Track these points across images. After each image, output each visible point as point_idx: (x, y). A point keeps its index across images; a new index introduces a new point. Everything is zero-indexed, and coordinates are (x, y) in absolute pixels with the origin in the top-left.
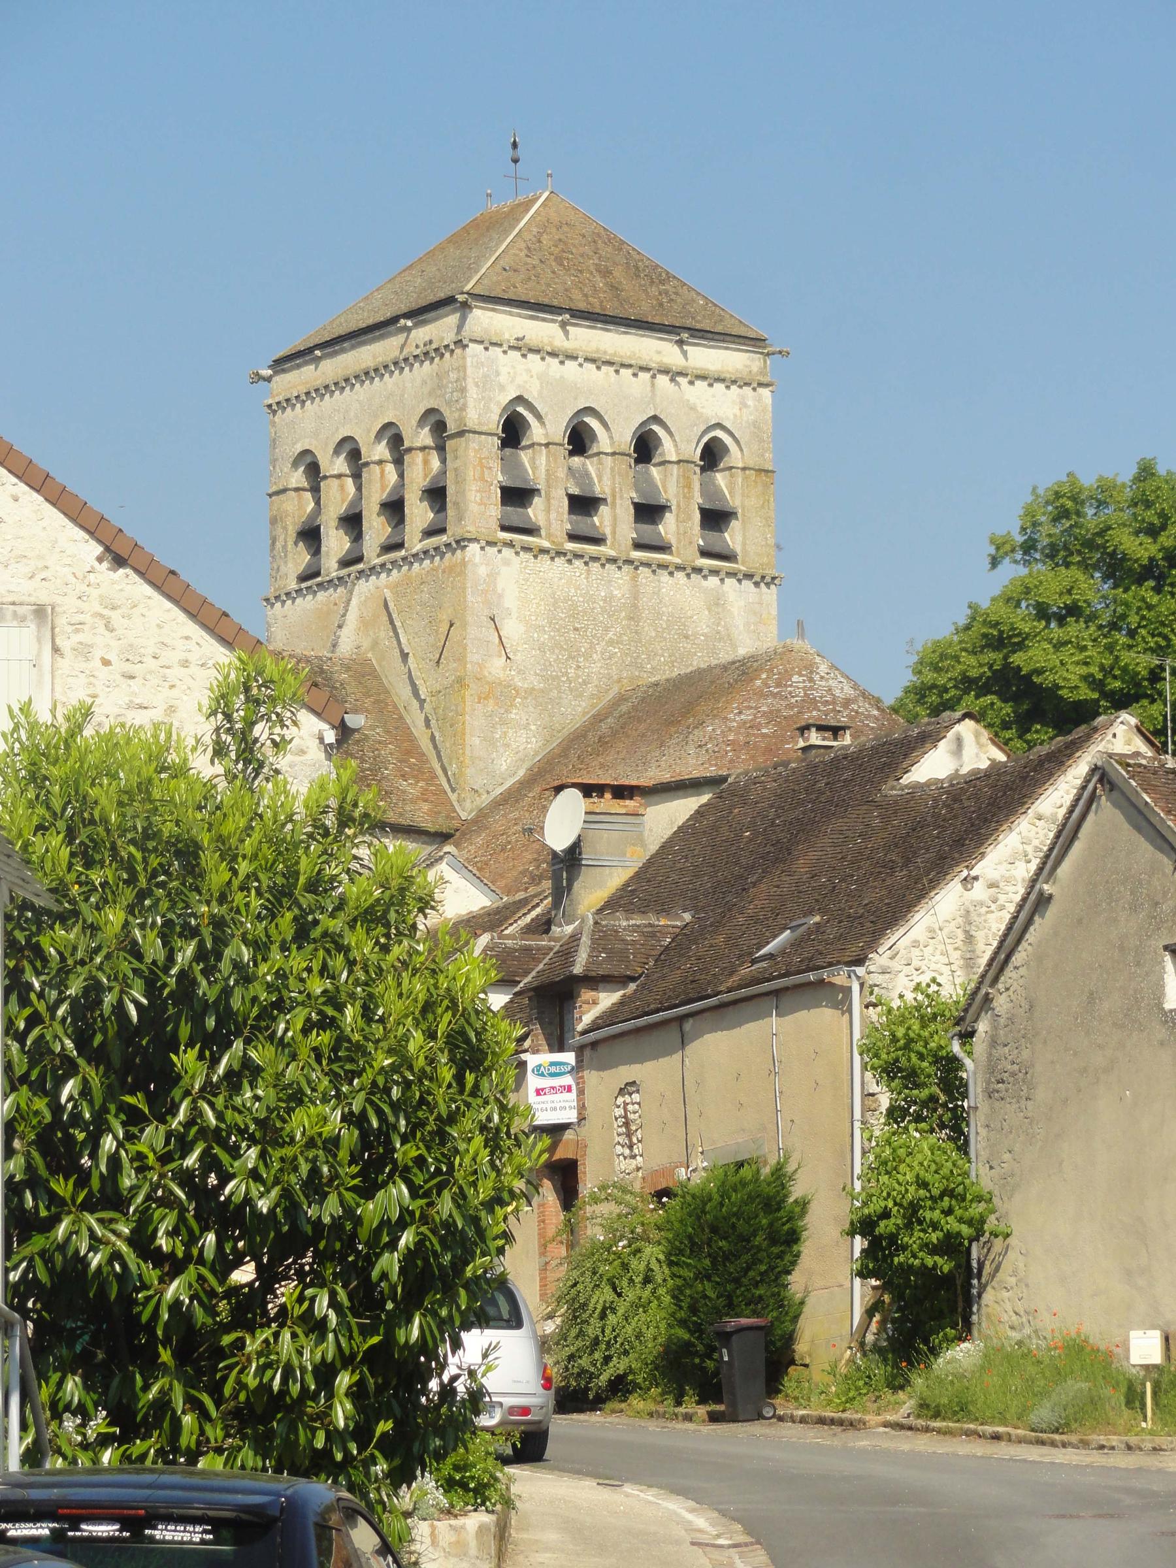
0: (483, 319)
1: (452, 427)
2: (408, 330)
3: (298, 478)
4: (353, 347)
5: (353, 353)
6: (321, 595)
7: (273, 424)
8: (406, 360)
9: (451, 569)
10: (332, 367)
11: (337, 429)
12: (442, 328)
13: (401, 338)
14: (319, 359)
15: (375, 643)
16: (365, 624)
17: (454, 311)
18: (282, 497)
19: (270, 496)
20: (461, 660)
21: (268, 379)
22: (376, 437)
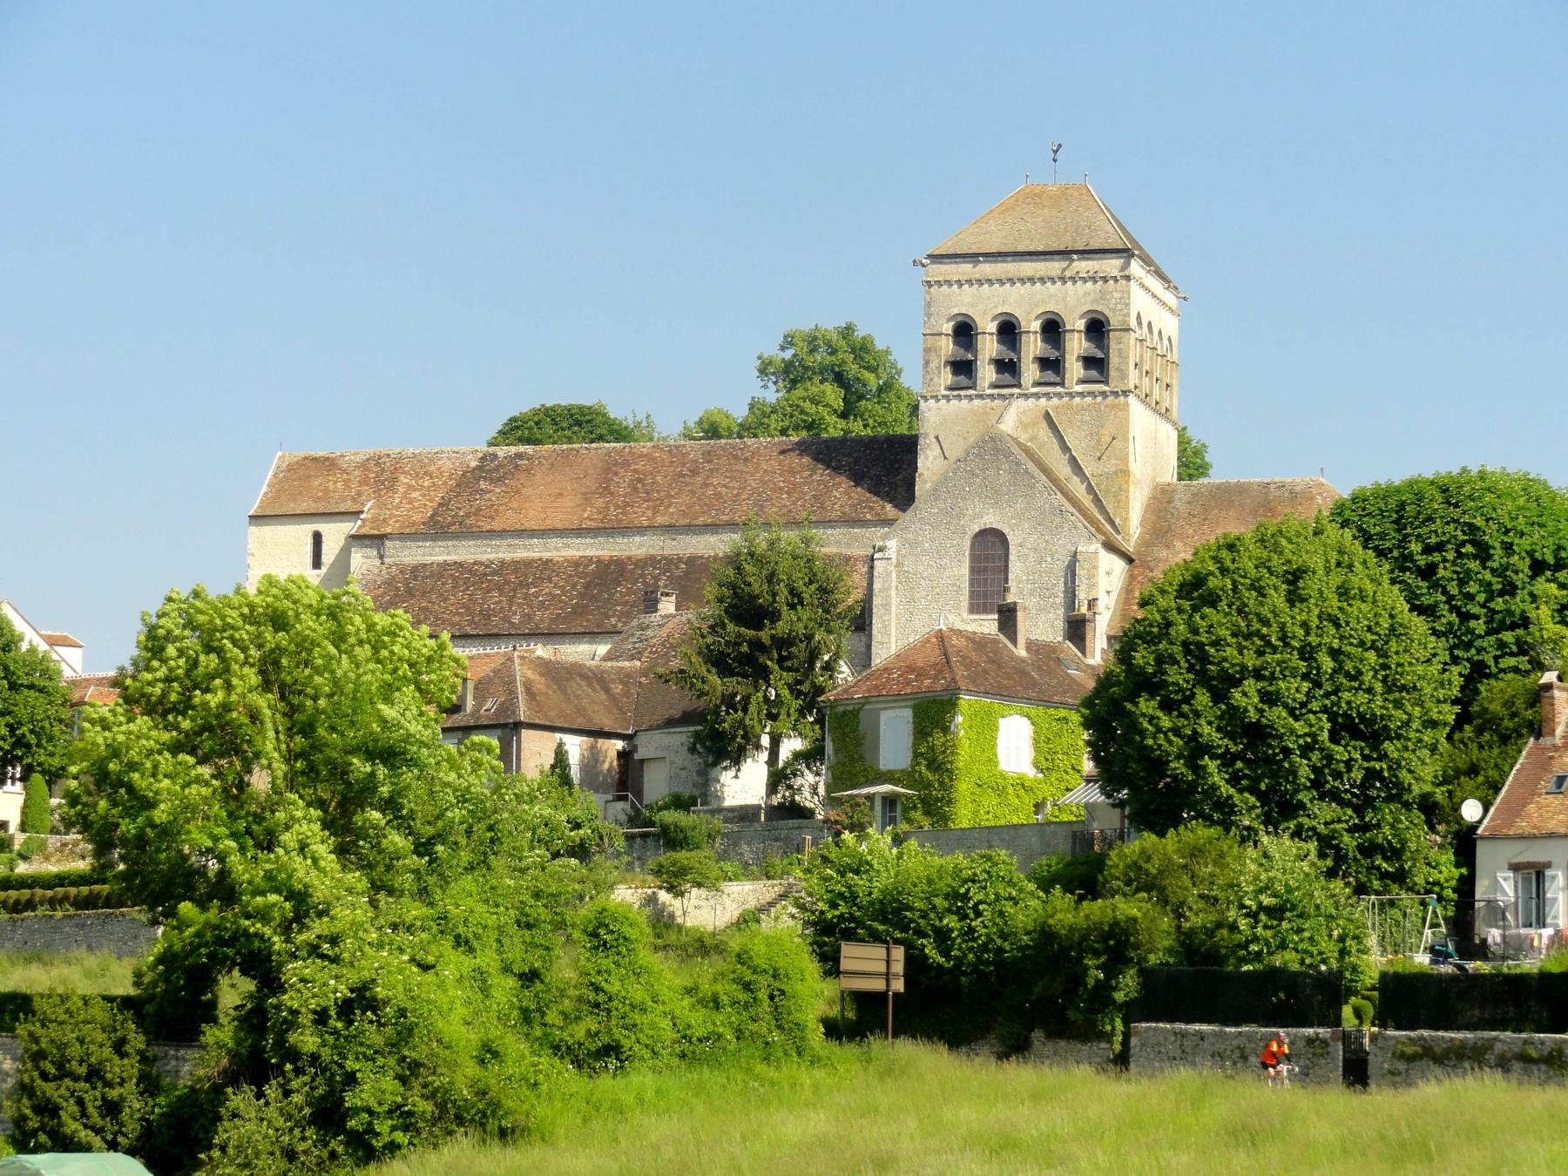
0: (1135, 267)
1: (1115, 322)
3: (948, 328)
6: (976, 402)
8: (1073, 279)
9: (1113, 406)
10: (987, 269)
12: (1112, 265)
13: (1064, 264)
15: (1033, 438)
16: (1023, 426)
20: (1125, 459)
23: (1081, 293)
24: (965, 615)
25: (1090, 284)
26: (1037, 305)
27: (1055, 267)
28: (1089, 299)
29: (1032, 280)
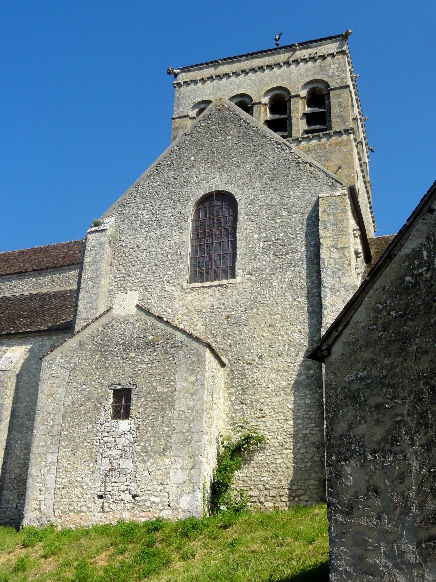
2: (295, 51)
4: (247, 59)
5: (248, 62)
7: (179, 91)
9: (337, 144)
11: (232, 91)
14: (219, 65)
17: (336, 41)
18: (184, 119)
19: (173, 119)
21: (176, 75)
22: (265, 93)
23: (303, 70)
24: (185, 284)
25: (310, 64)
26: (266, 84)
27: (281, 57)
28: (310, 73)
29: (261, 68)
